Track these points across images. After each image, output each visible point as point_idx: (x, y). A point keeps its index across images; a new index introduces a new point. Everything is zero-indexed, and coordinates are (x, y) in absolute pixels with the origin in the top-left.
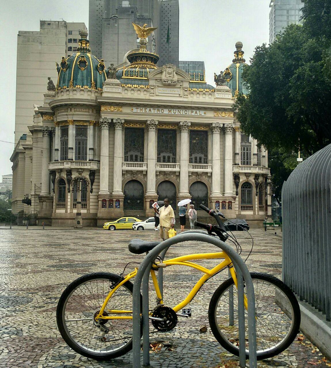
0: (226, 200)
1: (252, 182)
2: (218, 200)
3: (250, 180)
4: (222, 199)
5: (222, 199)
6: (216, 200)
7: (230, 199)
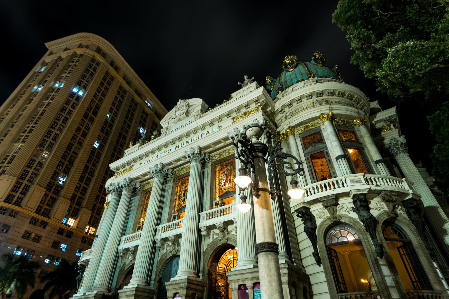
1: (350, 218)
2: (243, 279)
3: (344, 216)
6: (238, 280)
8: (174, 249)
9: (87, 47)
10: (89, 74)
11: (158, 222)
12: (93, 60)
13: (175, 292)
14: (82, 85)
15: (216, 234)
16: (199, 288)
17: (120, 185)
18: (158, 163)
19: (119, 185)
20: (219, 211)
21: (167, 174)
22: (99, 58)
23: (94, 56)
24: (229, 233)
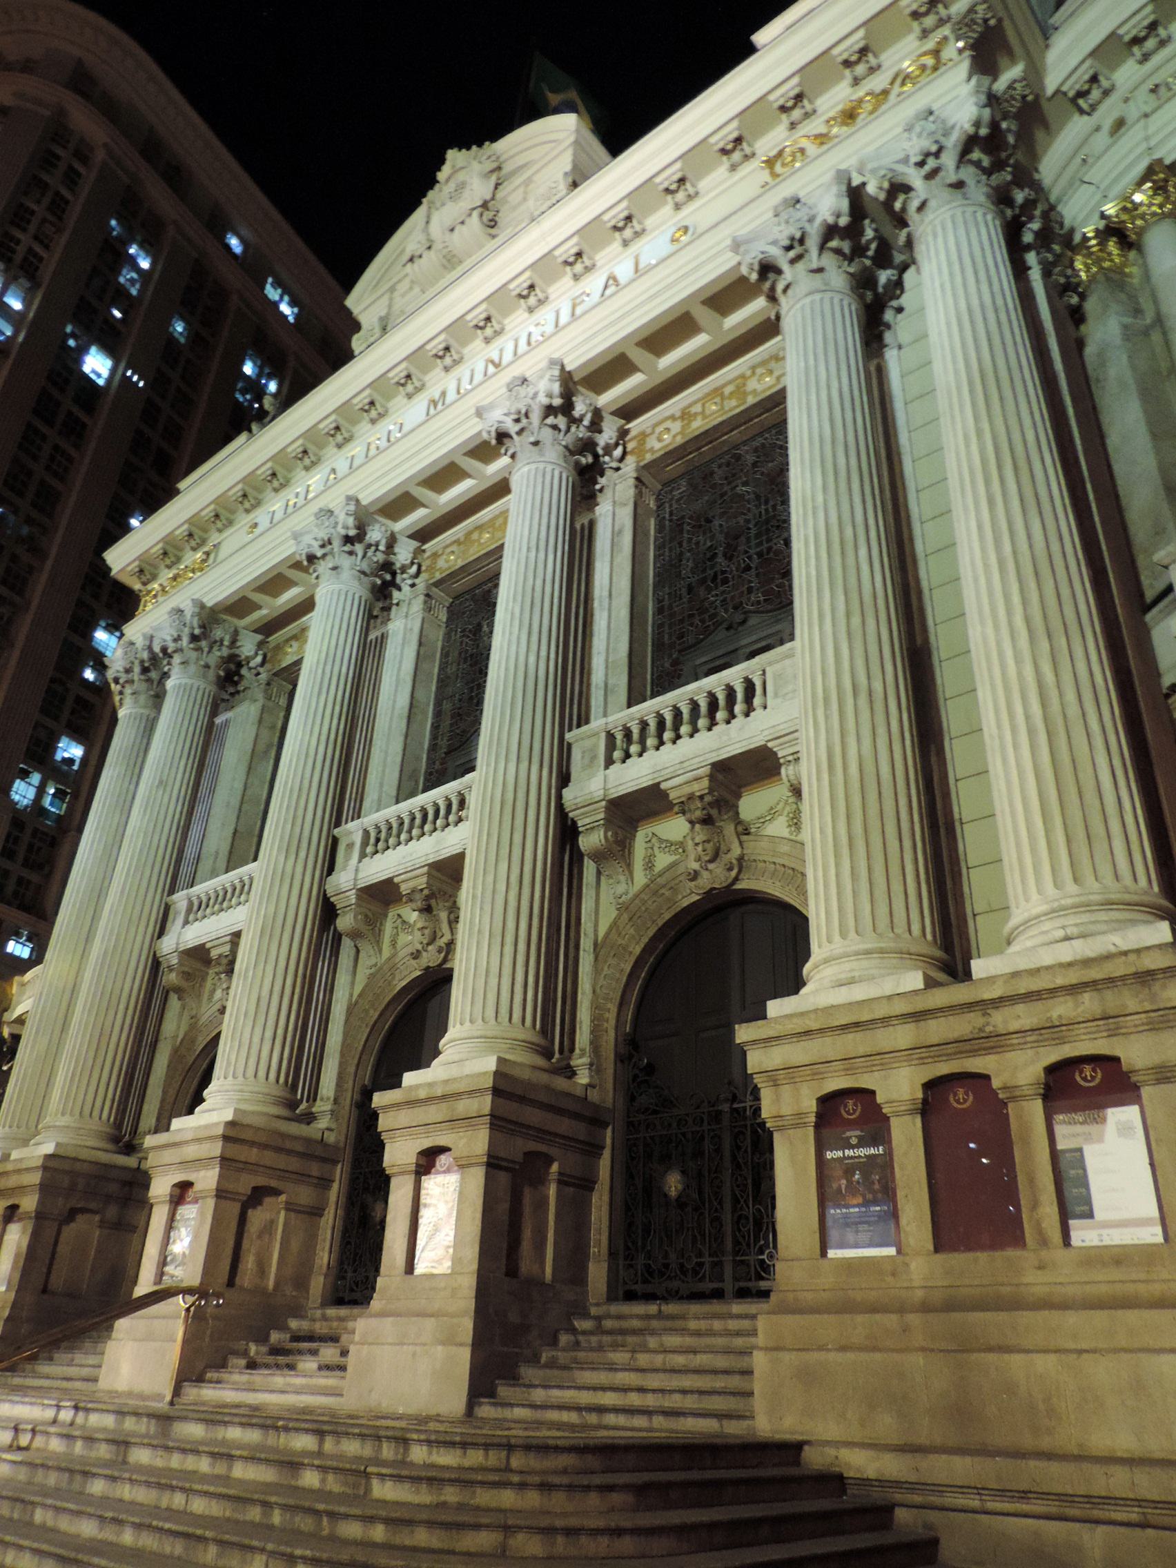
0: (991, 1042)
4: (903, 1036)
5: (903, 1036)
6: (816, 1068)
7: (1061, 1009)
8: (433, 940)
9: (27, 67)
10: (46, 201)
11: (343, 798)
12: (58, 130)
13: (427, 1143)
14: (18, 258)
15: (669, 845)
16: (564, 1126)
17: (157, 649)
18: (335, 500)
19: (150, 648)
20: (685, 710)
21: (387, 566)
22: (85, 121)
23: (61, 113)
24: (747, 832)
